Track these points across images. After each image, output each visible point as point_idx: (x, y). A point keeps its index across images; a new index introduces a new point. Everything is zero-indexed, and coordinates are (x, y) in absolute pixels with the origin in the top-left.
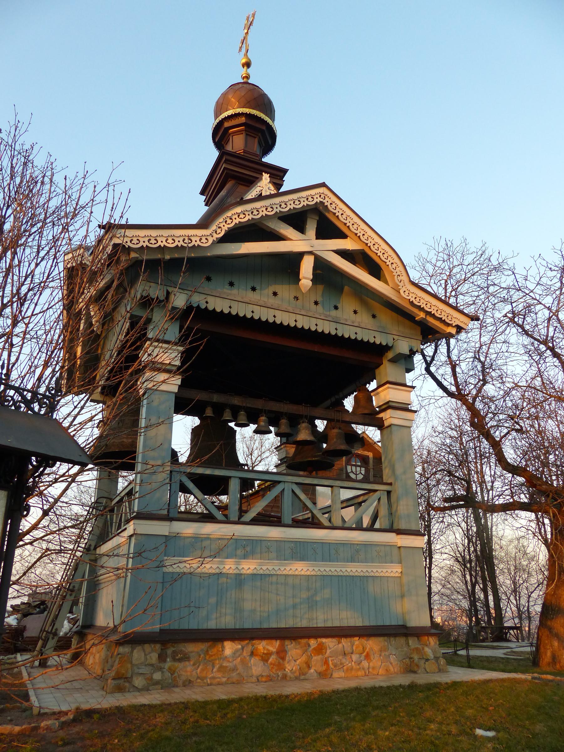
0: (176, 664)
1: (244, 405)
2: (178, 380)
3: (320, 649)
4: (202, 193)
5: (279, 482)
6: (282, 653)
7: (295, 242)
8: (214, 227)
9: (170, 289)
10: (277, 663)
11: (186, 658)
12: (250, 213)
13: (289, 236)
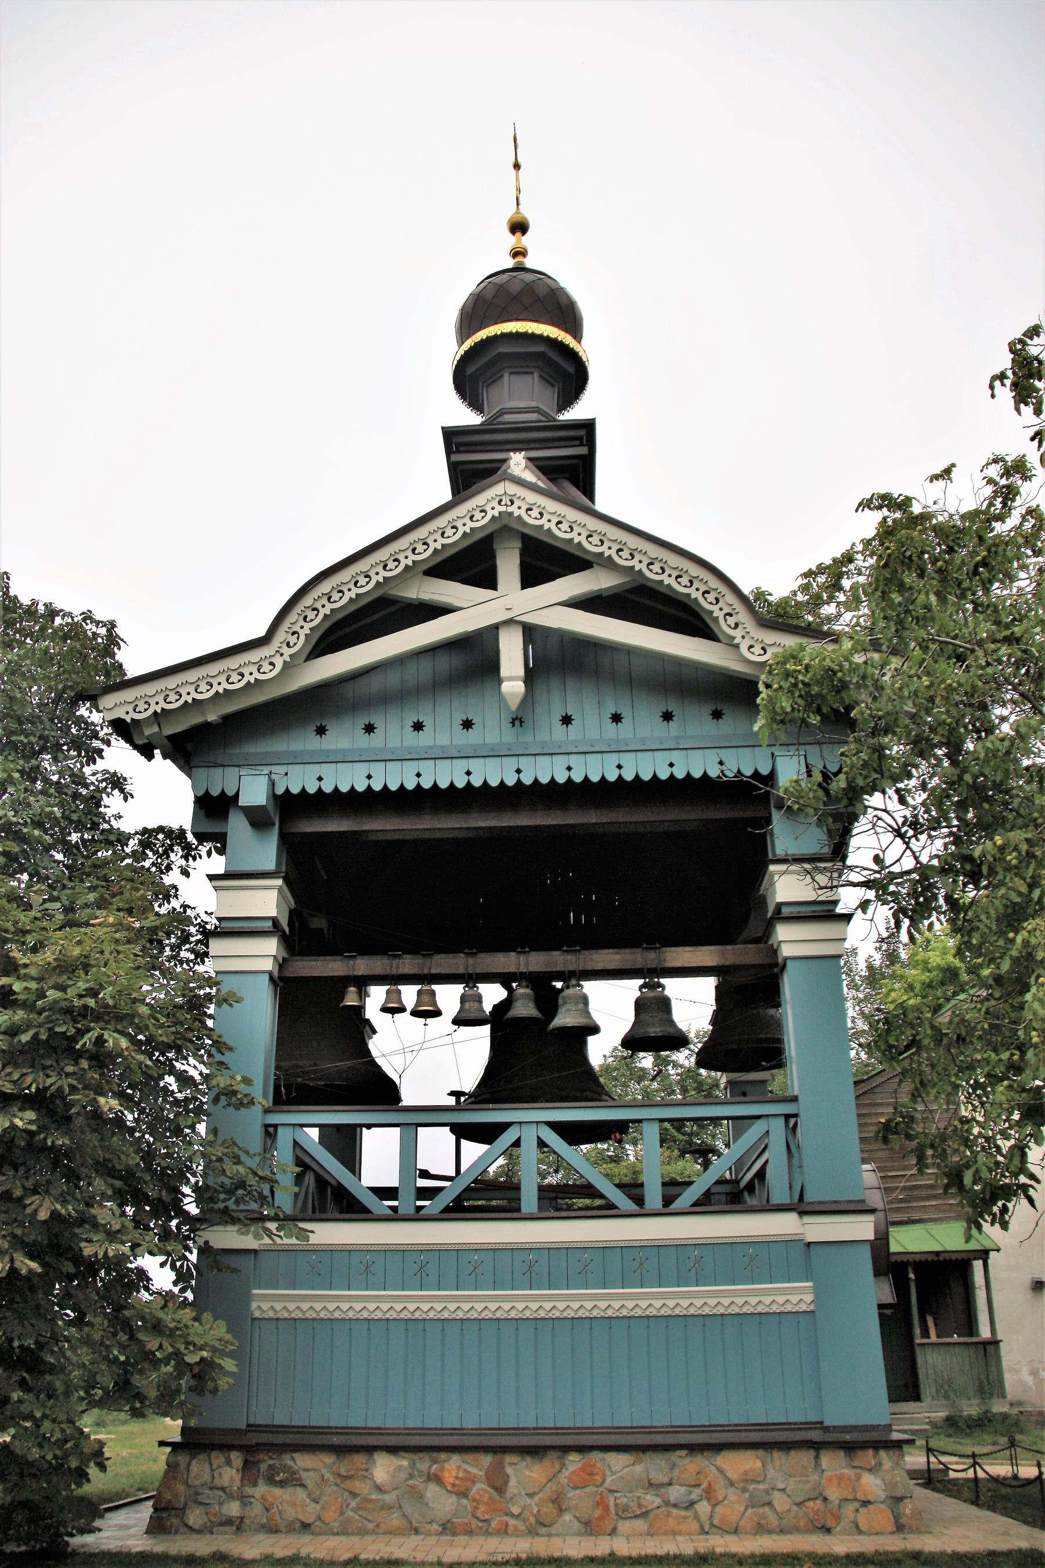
0: (277, 1491)
1: (426, 971)
2: (271, 946)
3: (588, 1476)
5: (508, 1125)
6: (498, 1483)
7: (471, 609)
10: (486, 1499)
11: (293, 1480)
12: (351, 585)
13: (457, 603)
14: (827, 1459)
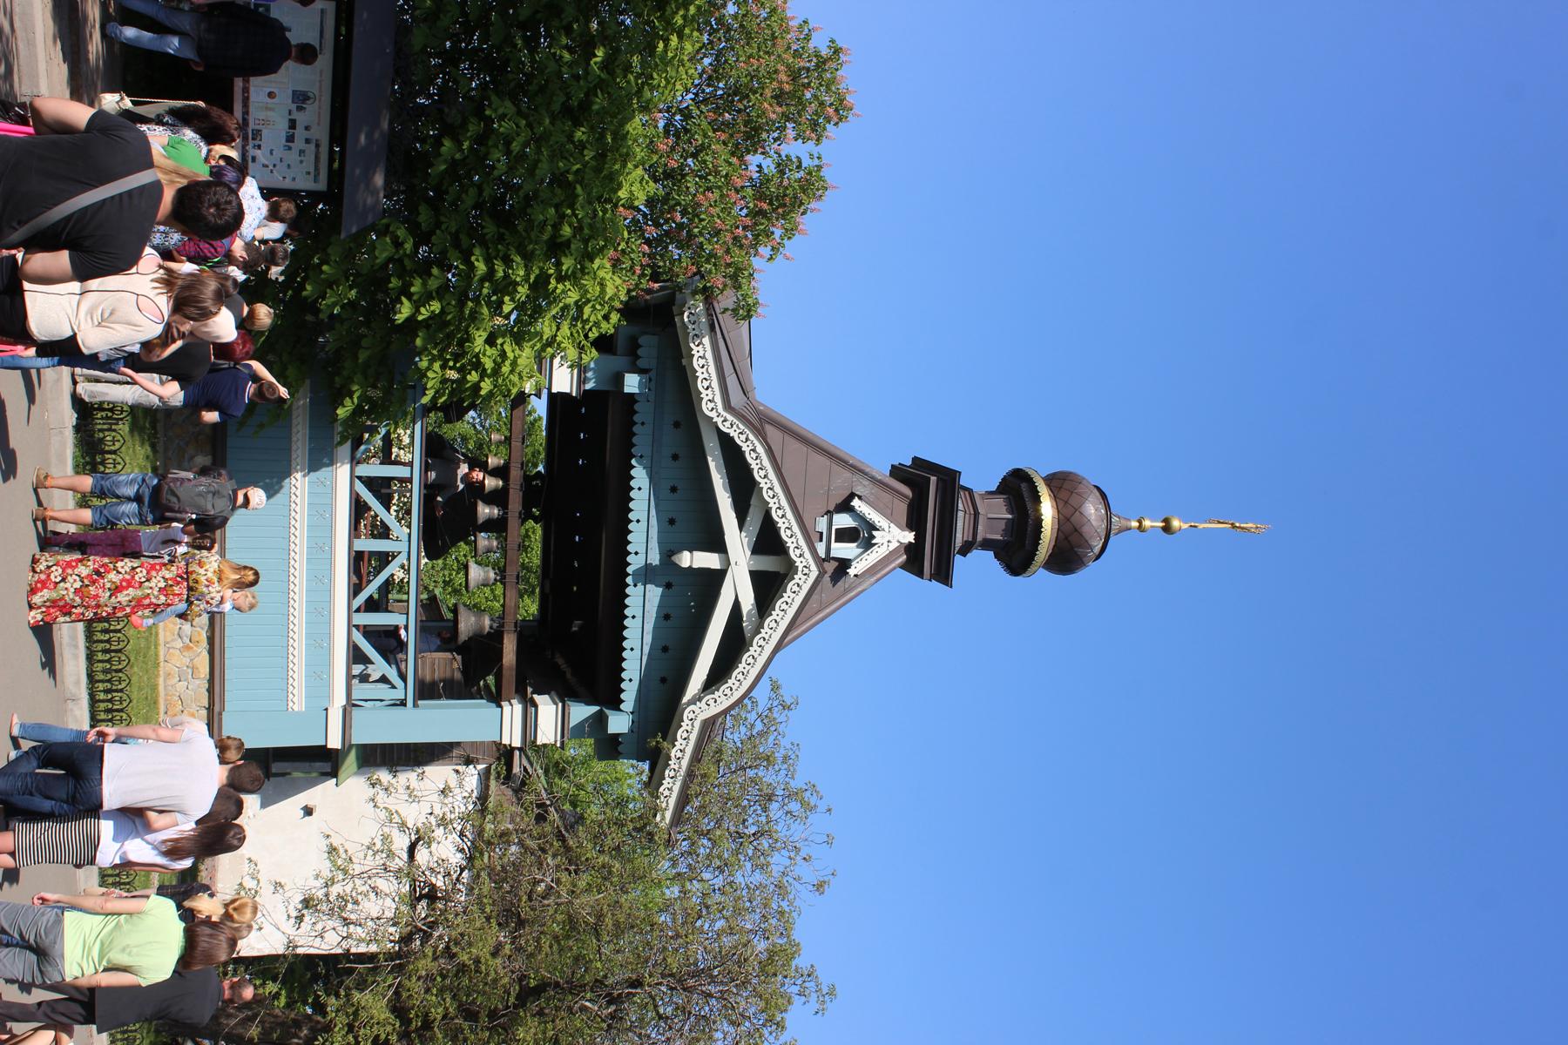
4: (915, 459)
7: (738, 541)
8: (730, 418)
9: (653, 374)
14: (204, 712)
